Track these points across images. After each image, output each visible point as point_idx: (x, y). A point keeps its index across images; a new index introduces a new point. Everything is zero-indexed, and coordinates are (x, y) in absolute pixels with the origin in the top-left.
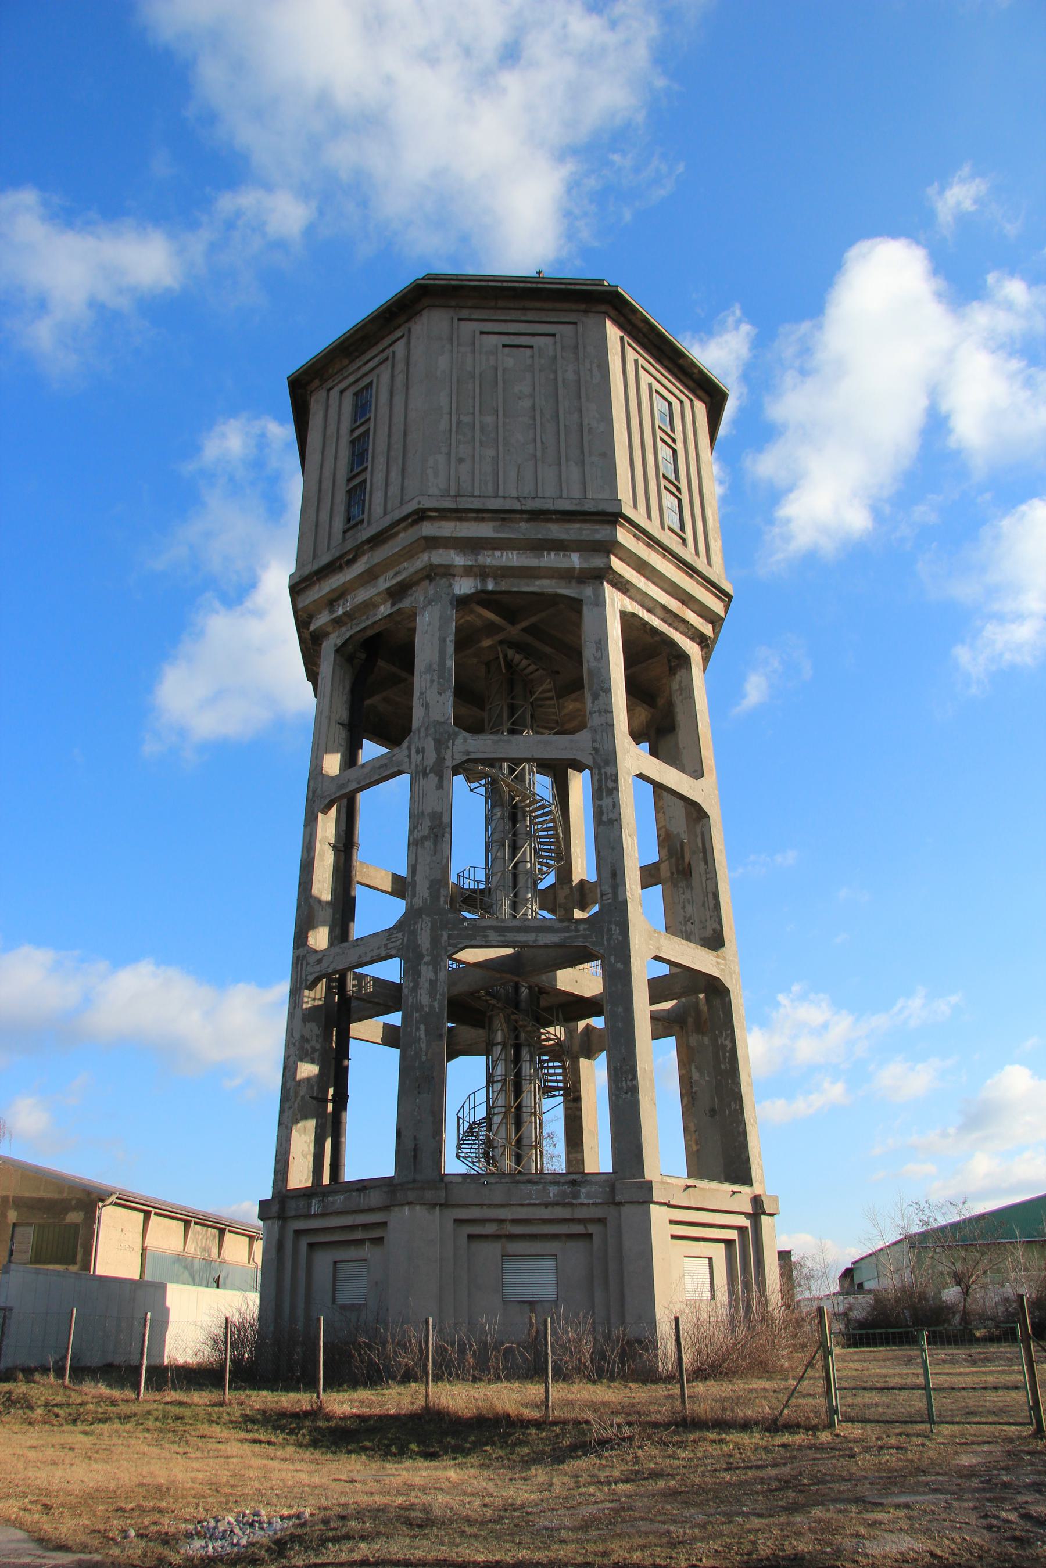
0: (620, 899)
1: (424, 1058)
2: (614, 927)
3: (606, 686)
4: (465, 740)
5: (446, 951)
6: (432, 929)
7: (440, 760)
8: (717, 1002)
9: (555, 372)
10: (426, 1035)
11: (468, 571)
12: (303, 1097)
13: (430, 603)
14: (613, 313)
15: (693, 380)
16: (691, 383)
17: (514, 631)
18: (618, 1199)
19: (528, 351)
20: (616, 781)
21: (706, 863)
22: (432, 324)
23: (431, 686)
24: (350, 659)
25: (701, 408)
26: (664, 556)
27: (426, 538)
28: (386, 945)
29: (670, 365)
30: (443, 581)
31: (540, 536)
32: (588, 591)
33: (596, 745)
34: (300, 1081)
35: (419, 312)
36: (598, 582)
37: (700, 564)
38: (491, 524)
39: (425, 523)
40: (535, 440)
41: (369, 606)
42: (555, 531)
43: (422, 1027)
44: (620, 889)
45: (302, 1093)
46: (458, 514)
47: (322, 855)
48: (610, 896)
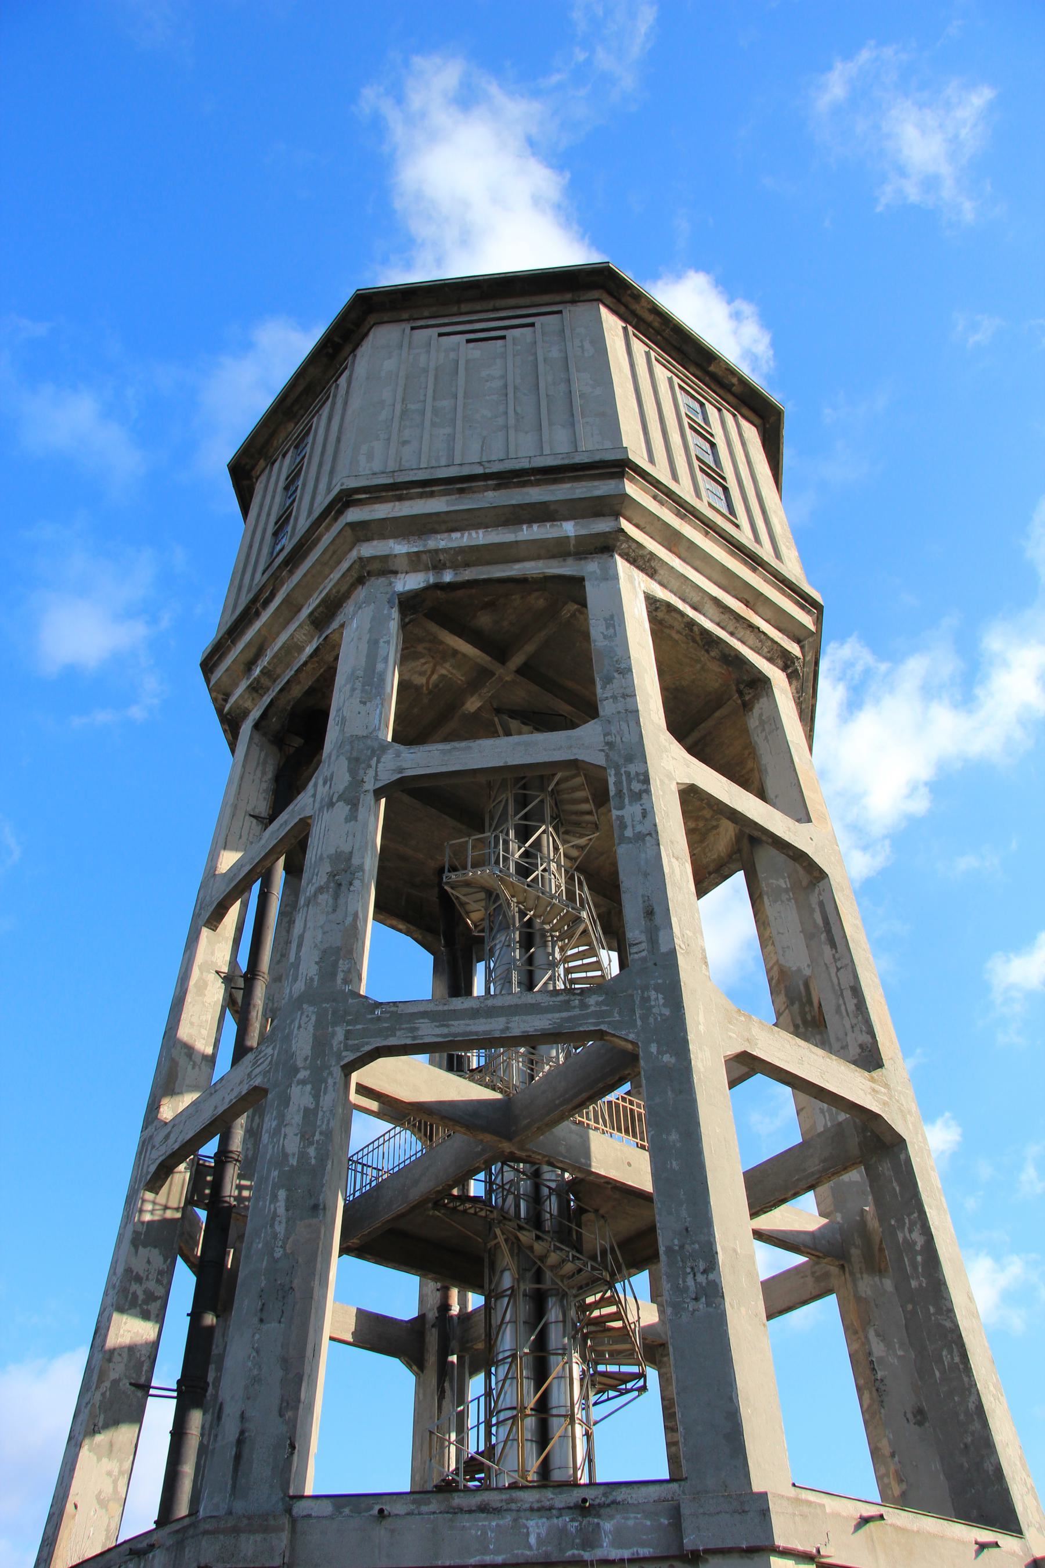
0: (663, 949)
1: (278, 1253)
2: (653, 994)
3: (623, 666)
4: (398, 755)
5: (339, 1057)
6: (316, 1027)
7: (357, 783)
8: (885, 1168)
9: (536, 353)
10: (287, 1210)
11: (415, 562)
12: (115, 1383)
13: (360, 608)
14: (609, 300)
15: (734, 395)
16: (730, 398)
17: (506, 672)
18: (691, 1541)
19: (500, 342)
20: (647, 781)
21: (833, 945)
22: (383, 349)
23: (351, 696)
24: (278, 741)
25: (751, 433)
26: (707, 534)
27: (352, 525)
28: (249, 1075)
29: (699, 373)
30: (382, 580)
31: (514, 502)
32: (590, 567)
33: (609, 738)
34: (112, 1351)
35: (366, 335)
36: (605, 556)
37: (765, 552)
38: (444, 499)
39: (351, 509)
40: (506, 413)
41: (291, 648)
42: (535, 494)
43: (282, 1194)
44: (662, 935)
45: (113, 1375)
46: (397, 490)
47: (202, 987)
48: (644, 946)
